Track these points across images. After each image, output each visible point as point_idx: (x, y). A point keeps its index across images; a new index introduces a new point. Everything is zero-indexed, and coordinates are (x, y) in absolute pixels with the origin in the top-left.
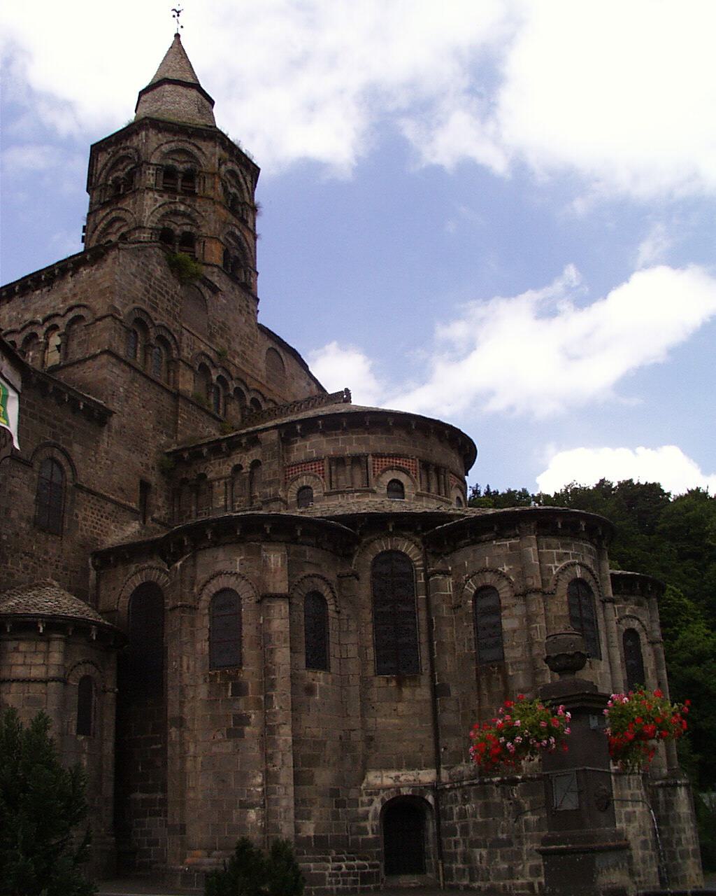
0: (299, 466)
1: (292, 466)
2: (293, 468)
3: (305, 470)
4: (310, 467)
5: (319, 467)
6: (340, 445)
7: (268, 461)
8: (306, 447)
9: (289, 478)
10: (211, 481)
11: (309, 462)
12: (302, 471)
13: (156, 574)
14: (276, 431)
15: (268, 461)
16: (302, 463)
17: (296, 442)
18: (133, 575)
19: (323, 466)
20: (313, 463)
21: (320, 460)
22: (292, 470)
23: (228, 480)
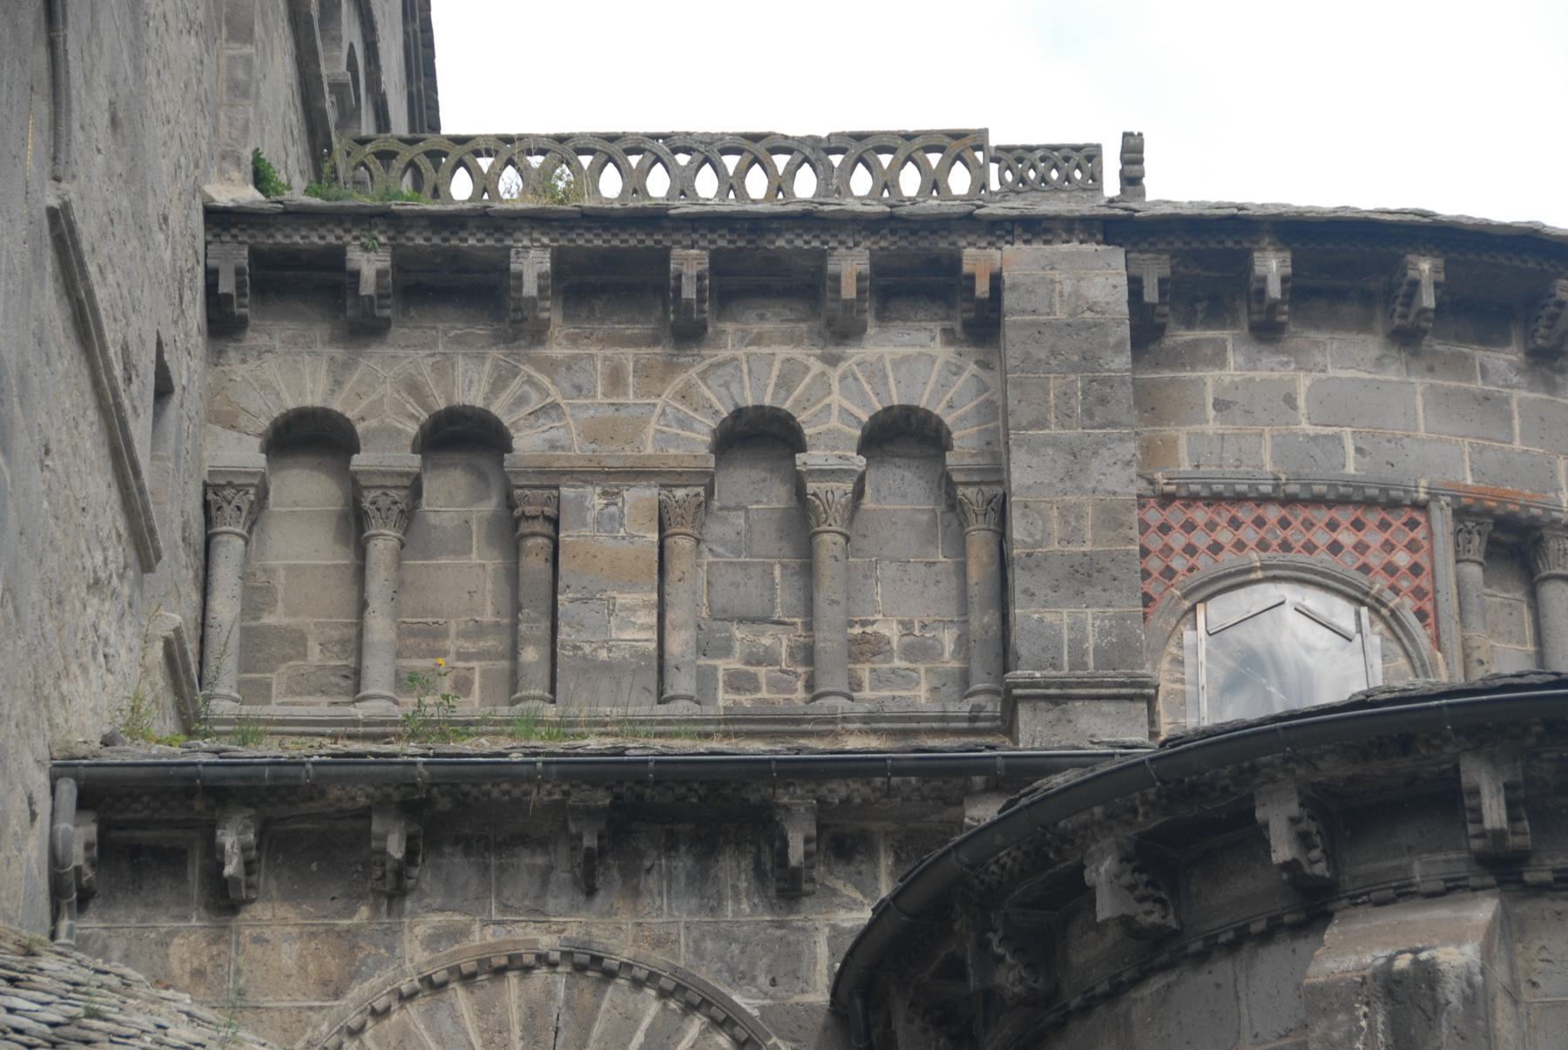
0: (1245, 514)
1: (1192, 499)
2: (1200, 515)
3: (1286, 546)
4: (1321, 538)
5: (1388, 547)
6: (1517, 445)
7: (1054, 430)
8: (1290, 400)
9: (1169, 573)
10: (551, 477)
11: (1318, 501)
12: (1263, 545)
13: (631, 1020)
14: (1116, 257)
15: (1054, 430)
16: (1263, 500)
17: (1218, 360)
18: (405, 998)
19: (1412, 547)
20: (1344, 516)
21: (1394, 505)
22: (1189, 527)
23: (680, 493)
